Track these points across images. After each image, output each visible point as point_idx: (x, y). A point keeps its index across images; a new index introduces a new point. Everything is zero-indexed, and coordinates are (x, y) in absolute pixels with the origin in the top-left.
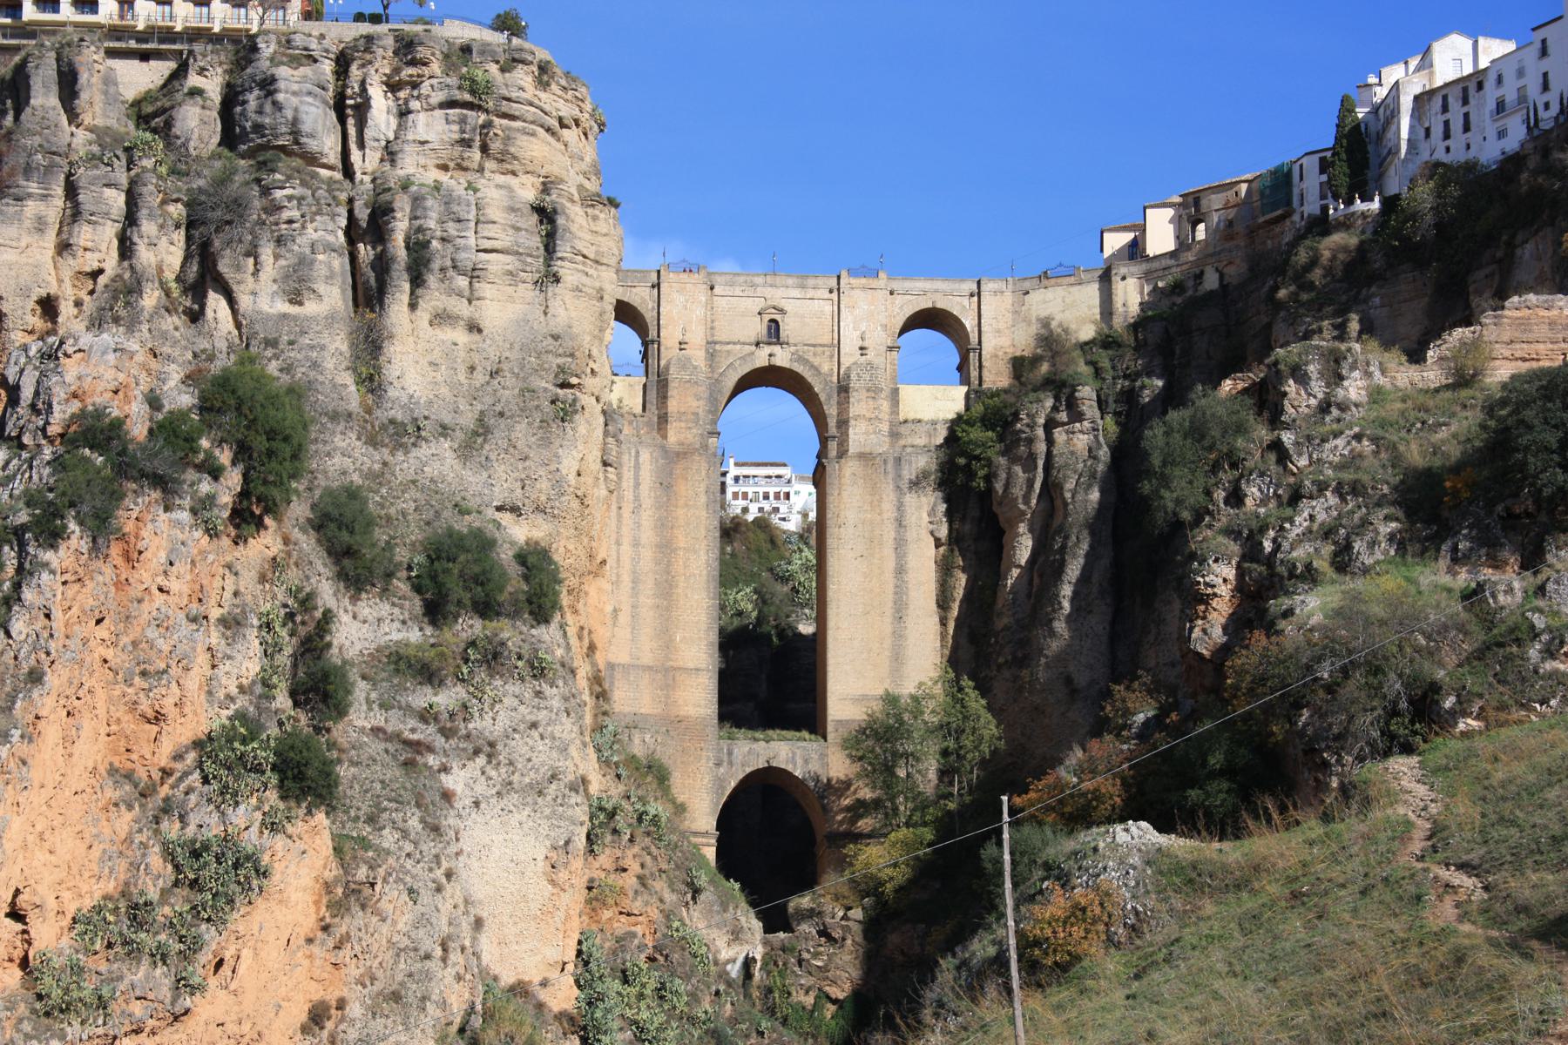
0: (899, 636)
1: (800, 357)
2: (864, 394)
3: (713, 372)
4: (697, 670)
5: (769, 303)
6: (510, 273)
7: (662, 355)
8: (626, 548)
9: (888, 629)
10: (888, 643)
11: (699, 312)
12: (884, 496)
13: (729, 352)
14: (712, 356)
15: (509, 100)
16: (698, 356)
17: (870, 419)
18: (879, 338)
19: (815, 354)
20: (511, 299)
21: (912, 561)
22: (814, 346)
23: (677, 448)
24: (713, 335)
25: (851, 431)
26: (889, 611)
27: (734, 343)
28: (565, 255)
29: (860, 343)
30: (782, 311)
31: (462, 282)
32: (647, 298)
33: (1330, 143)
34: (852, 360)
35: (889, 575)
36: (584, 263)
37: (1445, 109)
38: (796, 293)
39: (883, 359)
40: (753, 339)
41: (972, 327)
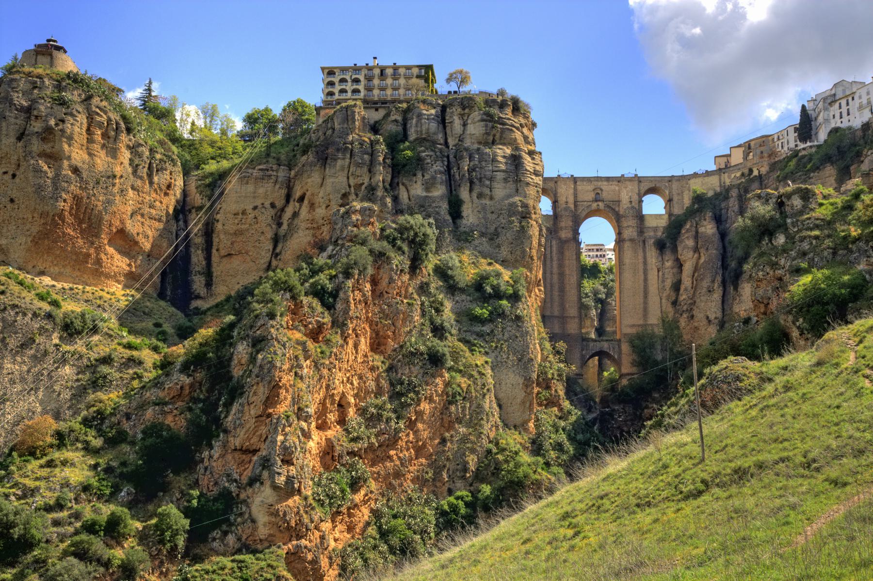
0: (645, 303)
9: (642, 301)
10: (642, 306)
11: (572, 191)
14: (576, 206)
16: (572, 206)
18: (635, 198)
20: (505, 188)
21: (650, 277)
26: (642, 294)
30: (602, 190)
31: (488, 182)
33: (798, 122)
35: (641, 282)
37: (840, 107)
38: (605, 183)
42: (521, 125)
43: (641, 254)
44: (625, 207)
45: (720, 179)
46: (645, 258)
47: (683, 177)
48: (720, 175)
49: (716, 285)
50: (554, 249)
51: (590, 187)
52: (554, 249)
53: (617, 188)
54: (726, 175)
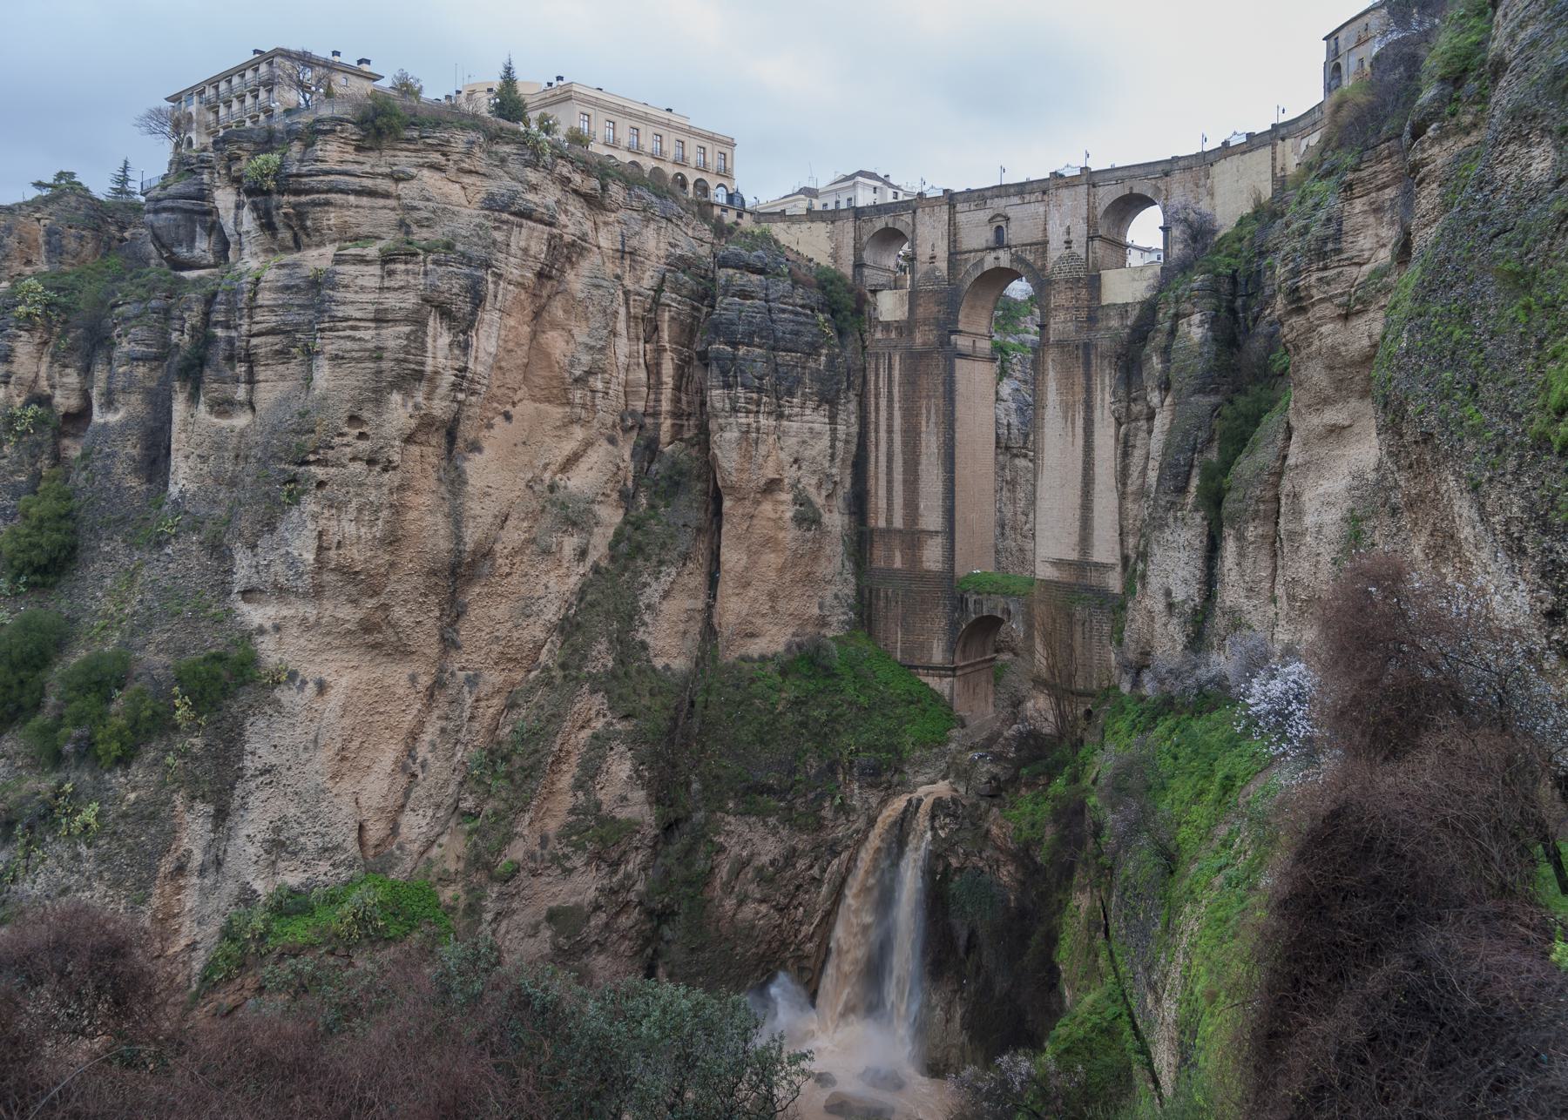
2: (1063, 286)
4: (937, 532)
6: (278, 352)
8: (883, 435)
13: (966, 260)
15: (299, 175)
16: (942, 265)
22: (1031, 245)
25: (1052, 321)
26: (1079, 486)
27: (970, 252)
28: (323, 326)
29: (1065, 238)
30: (1007, 219)
34: (1058, 254)
36: (353, 328)
38: (1016, 200)
39: (1084, 250)
42: (397, 178)
43: (1080, 380)
45: (1274, 159)
46: (1089, 390)
47: (1202, 156)
48: (1274, 146)
49: (1190, 499)
50: (896, 373)
51: (984, 215)
52: (896, 373)
53: (1042, 209)
54: (1289, 142)
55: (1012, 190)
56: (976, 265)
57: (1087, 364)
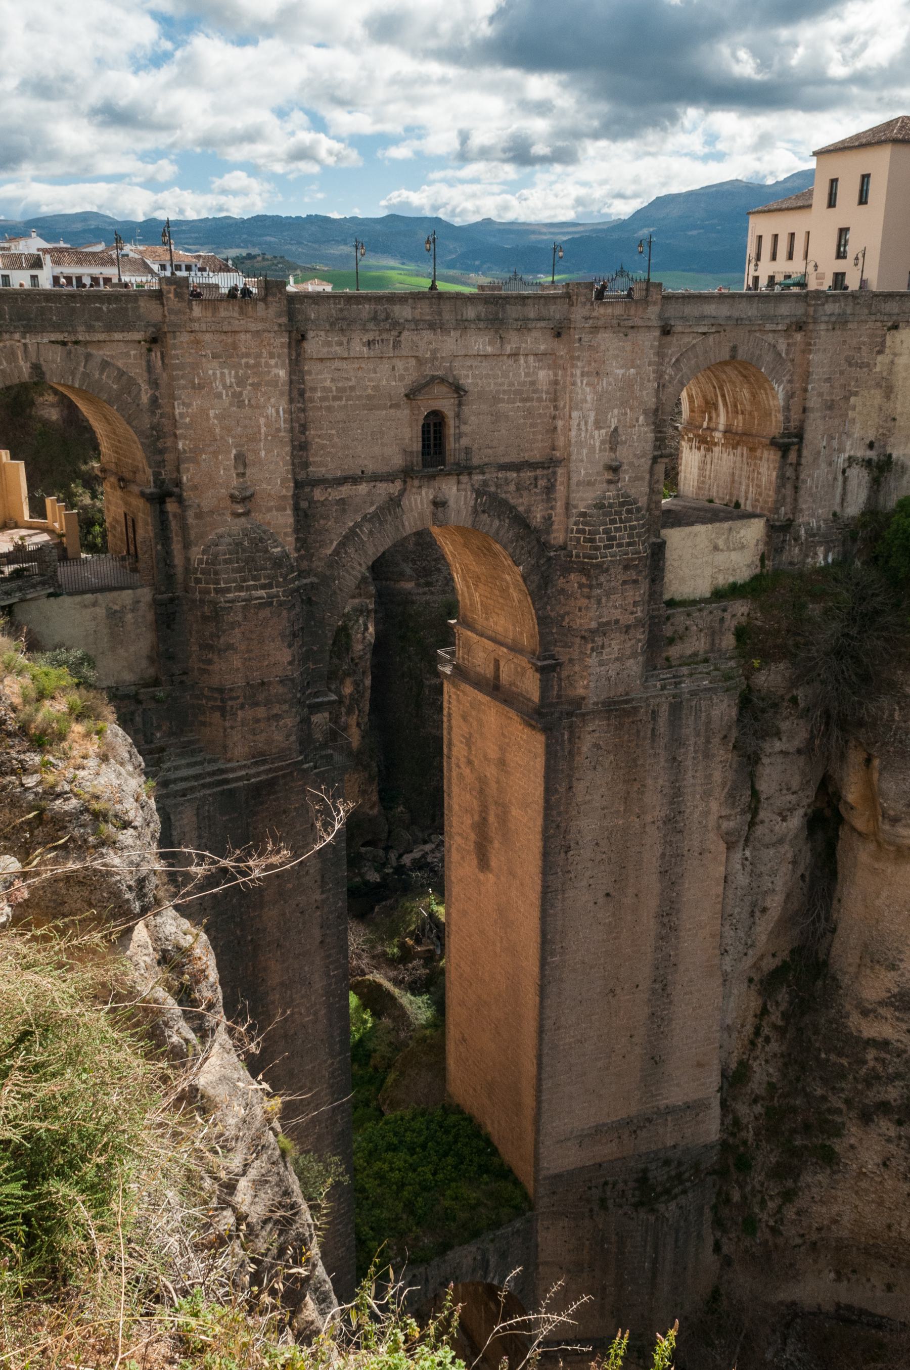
1: (493, 497)
3: (310, 557)
5: (429, 371)
7: (193, 534)
12: (650, 782)
13: (342, 502)
17: (628, 627)
19: (519, 488)
22: (517, 467)
23: (259, 774)
24: (306, 465)
25: (592, 661)
27: (354, 480)
32: (138, 372)
38: (481, 343)
40: (398, 461)
41: (790, 396)
44: (584, 499)
46: (676, 795)
53: (543, 376)
55: (470, 313)
56: (377, 518)
57: (677, 741)
